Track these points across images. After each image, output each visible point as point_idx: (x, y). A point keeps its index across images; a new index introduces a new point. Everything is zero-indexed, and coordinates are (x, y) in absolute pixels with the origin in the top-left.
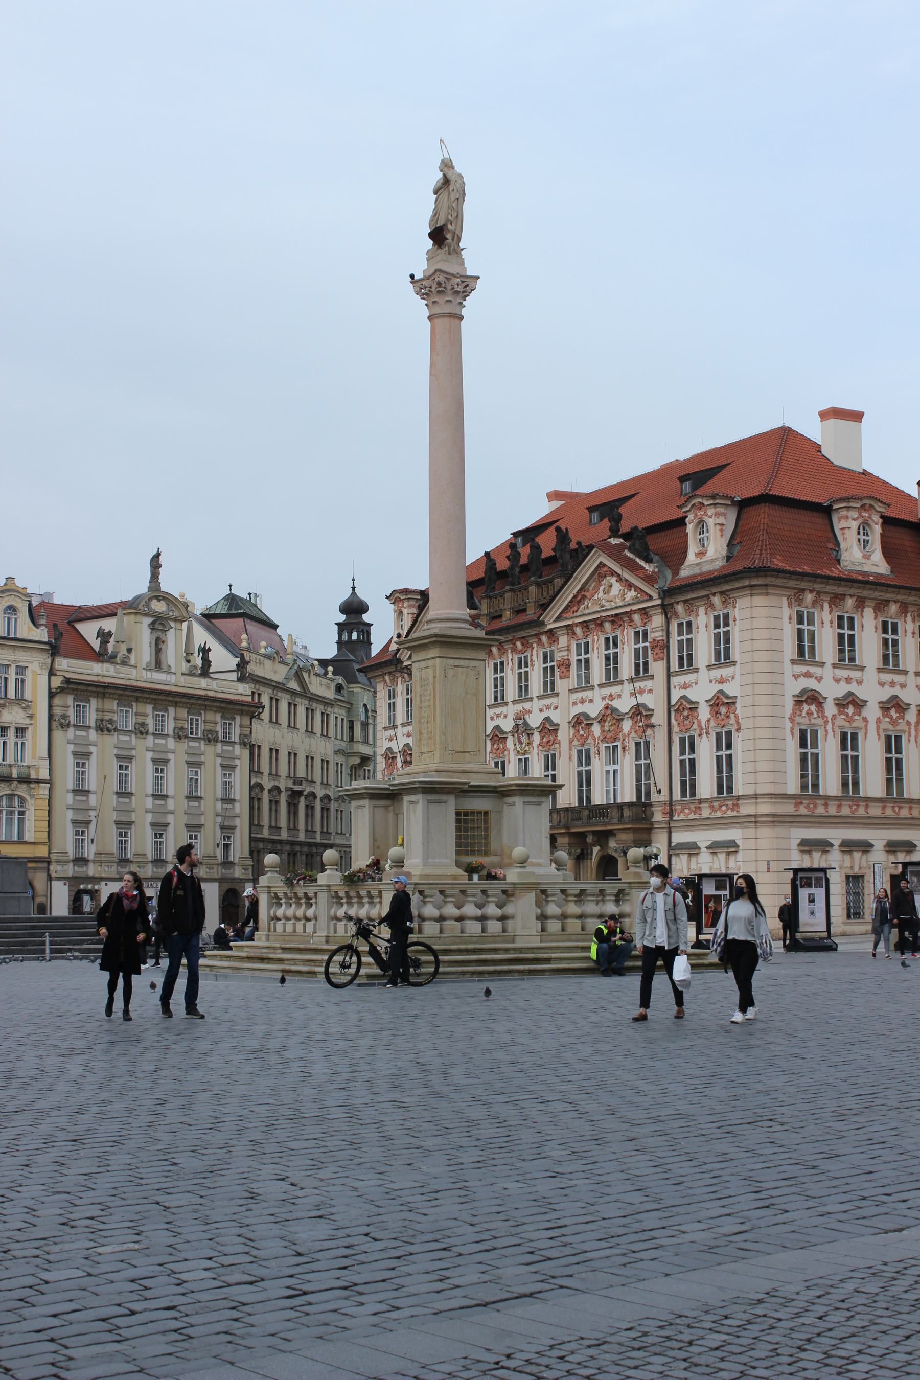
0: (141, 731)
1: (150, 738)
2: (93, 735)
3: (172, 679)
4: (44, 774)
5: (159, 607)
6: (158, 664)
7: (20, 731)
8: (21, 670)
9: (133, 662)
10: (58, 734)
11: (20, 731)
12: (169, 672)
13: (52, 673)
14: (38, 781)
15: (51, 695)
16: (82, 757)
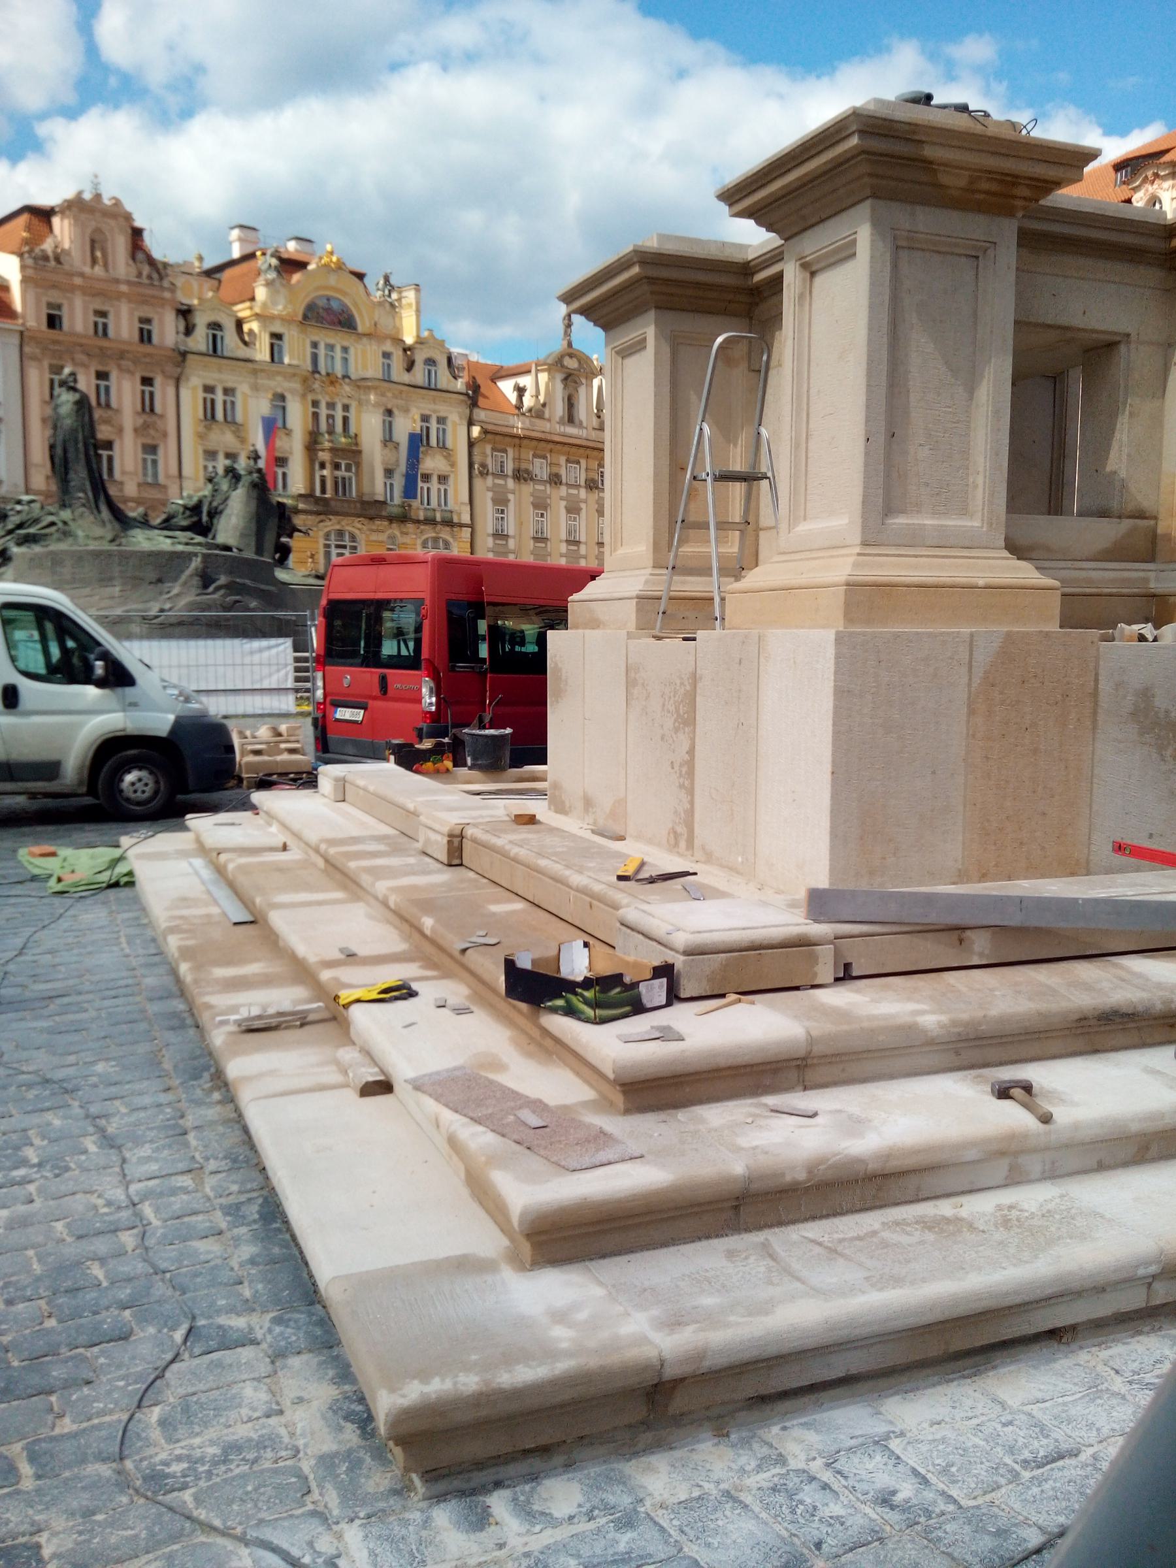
0: (555, 480)
1: (563, 489)
2: (510, 483)
3: (583, 433)
4: (466, 519)
5: (571, 364)
6: (571, 419)
7: (443, 479)
8: (441, 420)
9: (547, 415)
10: (478, 483)
11: (443, 479)
12: (580, 425)
13: (471, 423)
14: (461, 525)
15: (471, 444)
16: (501, 502)
